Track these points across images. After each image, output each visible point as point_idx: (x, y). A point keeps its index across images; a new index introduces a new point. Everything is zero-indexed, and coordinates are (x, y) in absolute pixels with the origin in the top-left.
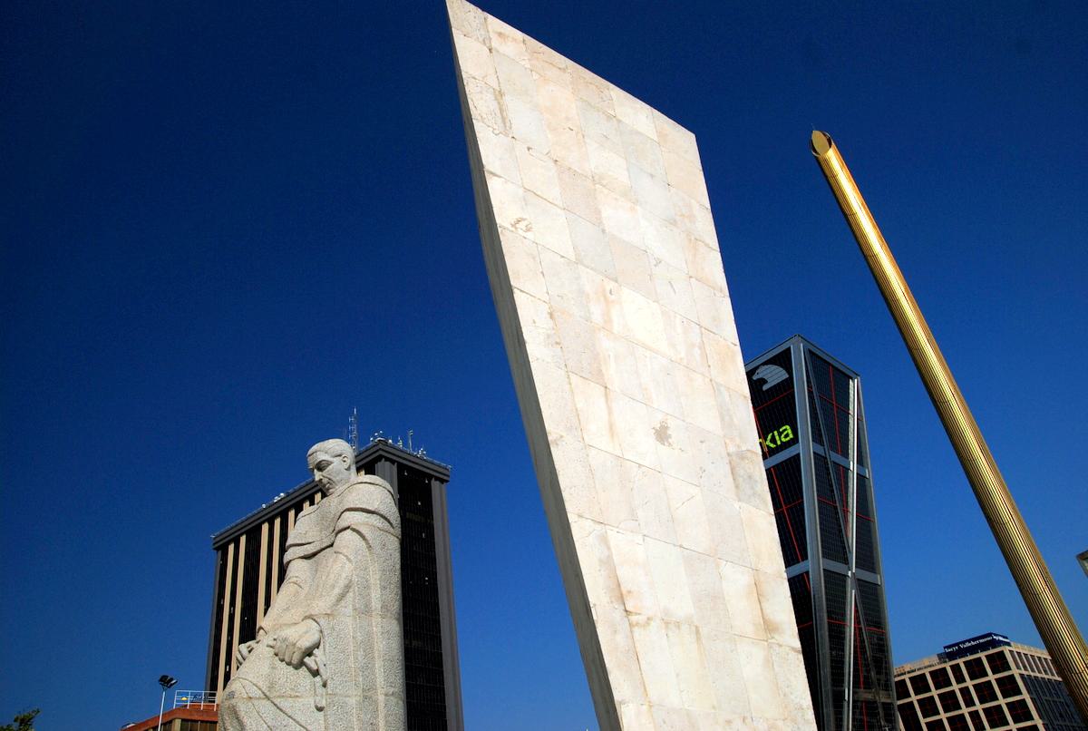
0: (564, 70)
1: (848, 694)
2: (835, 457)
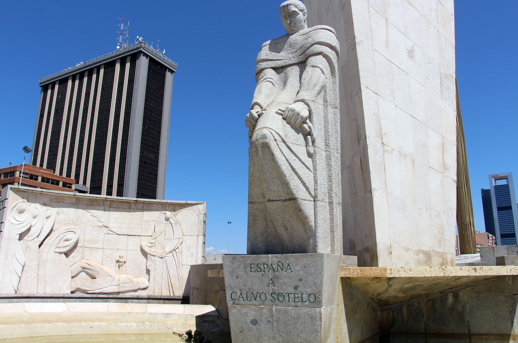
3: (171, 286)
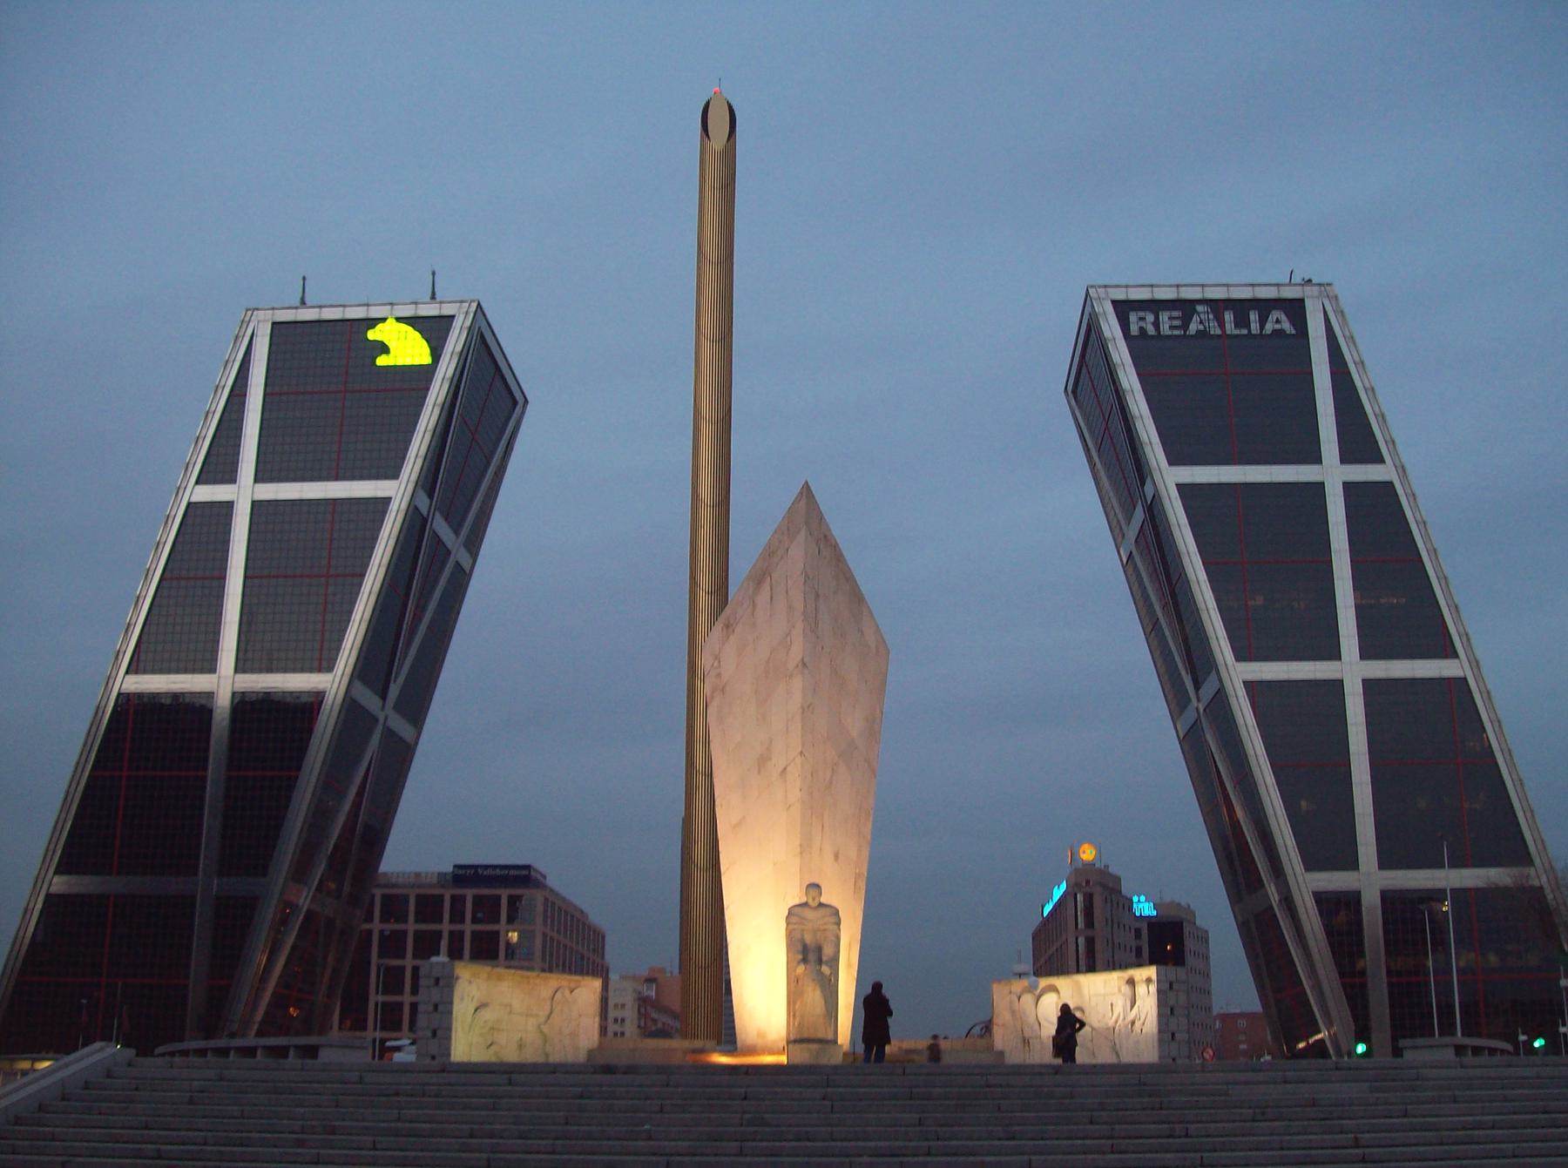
2: (440, 526)
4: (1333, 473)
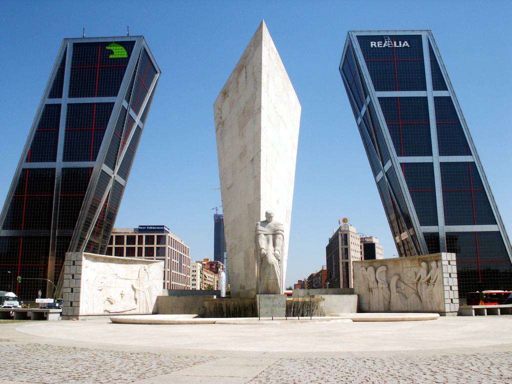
0: (282, 70)
1: (88, 237)
2: (131, 112)
3: (147, 308)
4: (430, 94)
